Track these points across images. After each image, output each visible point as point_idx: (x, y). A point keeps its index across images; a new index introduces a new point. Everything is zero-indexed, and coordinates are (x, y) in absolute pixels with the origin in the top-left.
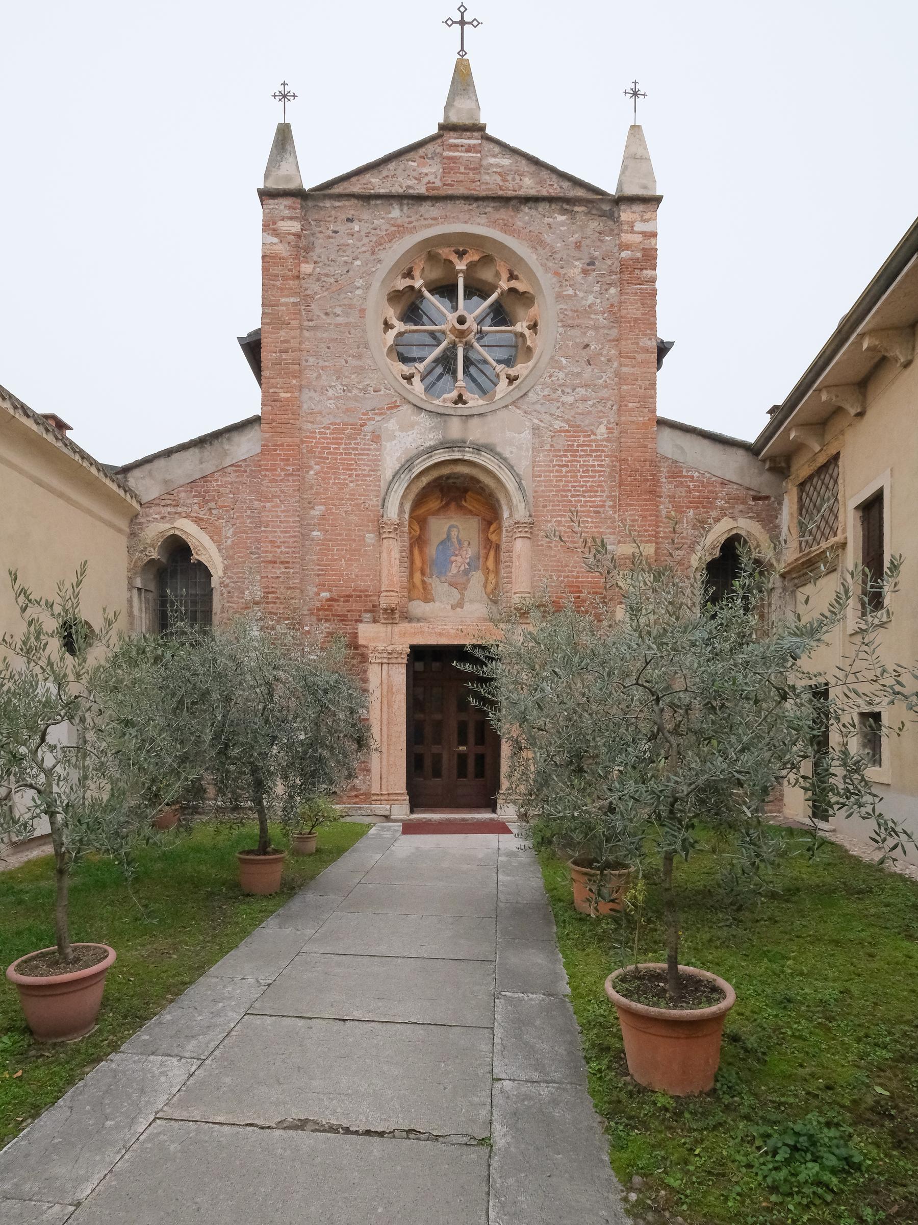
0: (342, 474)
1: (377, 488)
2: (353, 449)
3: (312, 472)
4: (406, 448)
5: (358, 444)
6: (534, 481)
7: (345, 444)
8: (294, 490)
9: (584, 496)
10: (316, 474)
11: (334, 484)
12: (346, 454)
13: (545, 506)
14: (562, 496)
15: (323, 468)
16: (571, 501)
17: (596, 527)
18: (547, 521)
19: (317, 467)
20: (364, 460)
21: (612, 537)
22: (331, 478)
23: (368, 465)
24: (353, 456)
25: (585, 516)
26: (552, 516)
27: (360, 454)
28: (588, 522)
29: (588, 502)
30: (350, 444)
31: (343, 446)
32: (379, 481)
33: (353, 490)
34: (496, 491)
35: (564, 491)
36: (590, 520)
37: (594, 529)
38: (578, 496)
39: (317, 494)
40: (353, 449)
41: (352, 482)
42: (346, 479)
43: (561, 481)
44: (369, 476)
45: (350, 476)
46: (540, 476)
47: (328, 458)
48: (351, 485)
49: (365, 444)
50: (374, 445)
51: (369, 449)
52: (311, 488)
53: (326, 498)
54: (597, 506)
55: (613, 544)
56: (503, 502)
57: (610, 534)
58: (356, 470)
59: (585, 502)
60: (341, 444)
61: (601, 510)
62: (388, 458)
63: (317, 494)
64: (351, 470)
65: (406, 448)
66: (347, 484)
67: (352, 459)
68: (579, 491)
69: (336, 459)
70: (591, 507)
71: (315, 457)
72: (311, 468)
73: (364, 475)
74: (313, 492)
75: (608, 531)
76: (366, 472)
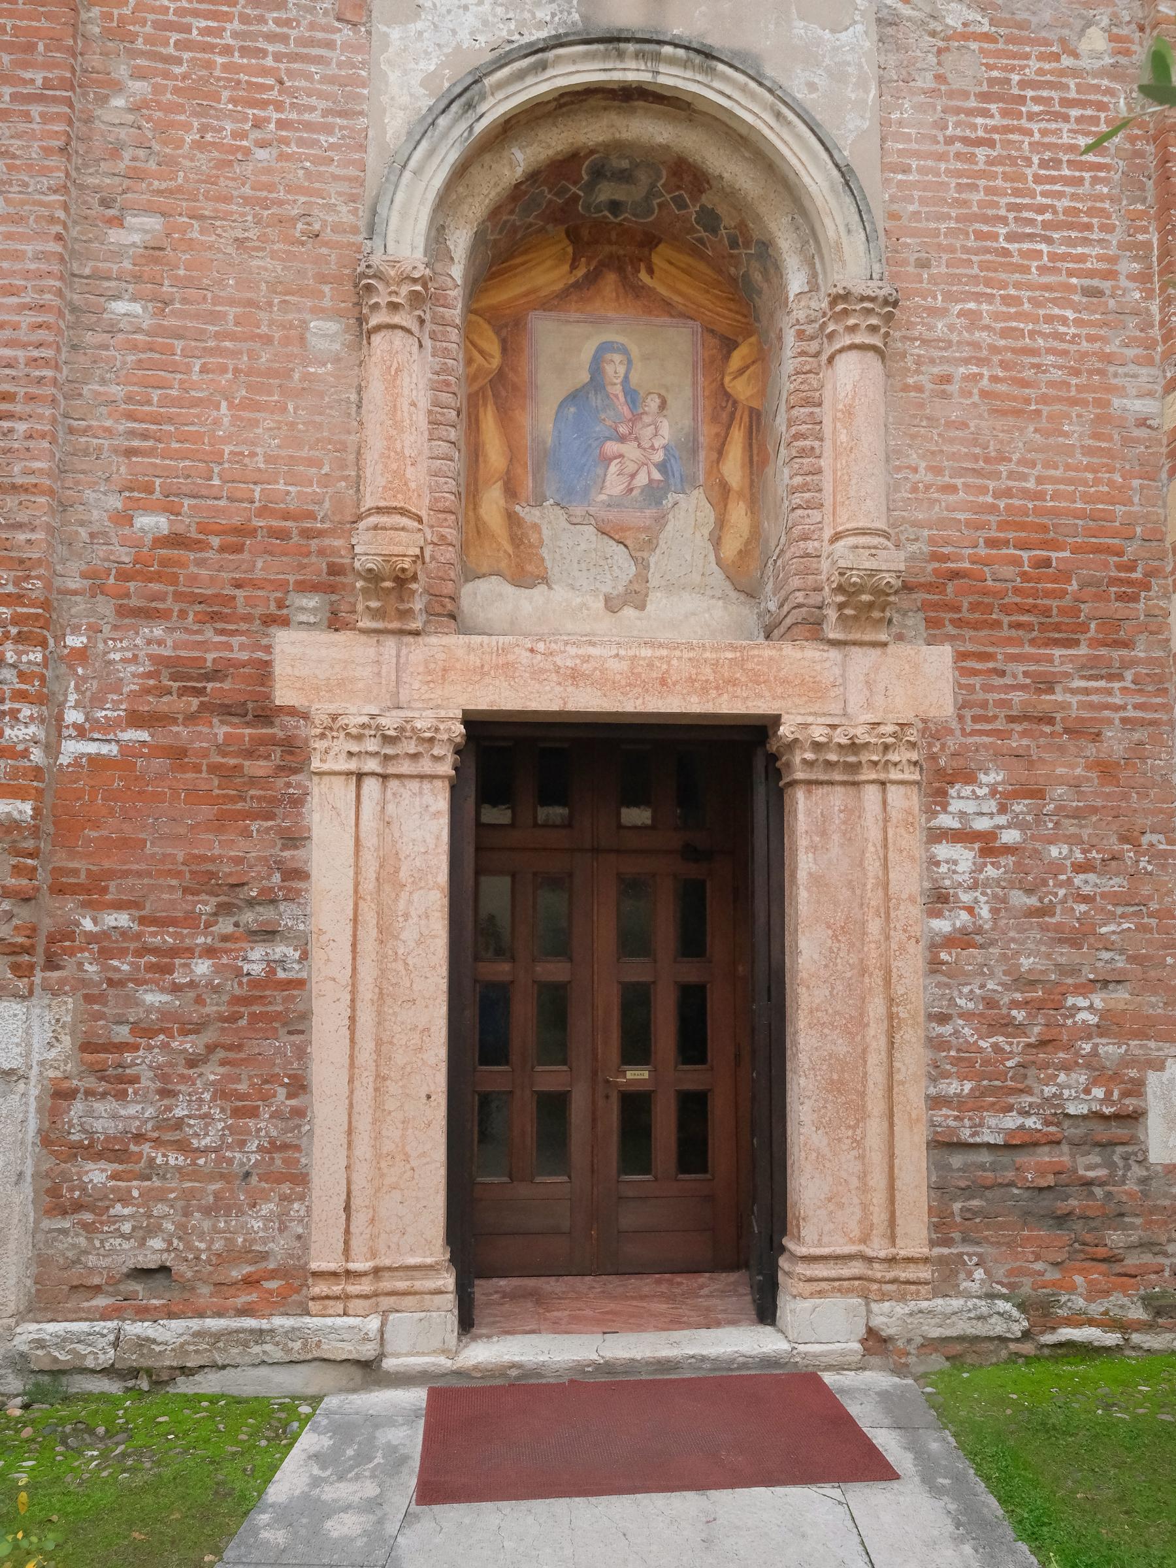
0: (231, 115)
1: (352, 171)
2: (271, 37)
3: (119, 102)
4: (459, 47)
5: (287, 23)
6: (886, 182)
7: (245, 19)
8: (47, 151)
9: (1049, 241)
10: (135, 109)
11: (200, 145)
12: (244, 51)
13: (923, 264)
14: (980, 235)
15: (156, 89)
16: (1006, 253)
17: (1091, 339)
18: (933, 312)
19: (140, 87)
20: (309, 77)
21: (1144, 371)
22: (187, 127)
23: (321, 95)
24: (269, 62)
25: (1054, 301)
26: (949, 297)
27: (294, 57)
28: (1064, 321)
29: (1064, 257)
30: (261, 20)
31: (236, 25)
32: (362, 148)
33: (268, 171)
34: (762, 209)
35: (986, 220)
36: (1070, 314)
37: (1085, 345)
38: (1031, 237)
39: (136, 175)
40: (271, 37)
41: (262, 145)
42: (243, 135)
43: (974, 187)
44: (328, 129)
45: (258, 124)
46: (906, 170)
47: (179, 61)
48: (261, 154)
49: (312, 26)
50: (347, 31)
51: (330, 45)
52: (115, 153)
53: (170, 192)
54: (1091, 274)
55: (1150, 394)
56: (786, 244)
57: (1136, 361)
58: (279, 107)
59: (1053, 257)
60: (228, 17)
61: (1106, 285)
62: (393, 76)
63: (136, 175)
64: (263, 104)
65: (459, 47)
66: (247, 152)
67: (265, 72)
68: (1031, 222)
69: (209, 65)
70: (1071, 273)
71: (133, 54)
72: (117, 87)
73: (309, 126)
74: (122, 166)
75: (1131, 352)
76: (315, 117)
